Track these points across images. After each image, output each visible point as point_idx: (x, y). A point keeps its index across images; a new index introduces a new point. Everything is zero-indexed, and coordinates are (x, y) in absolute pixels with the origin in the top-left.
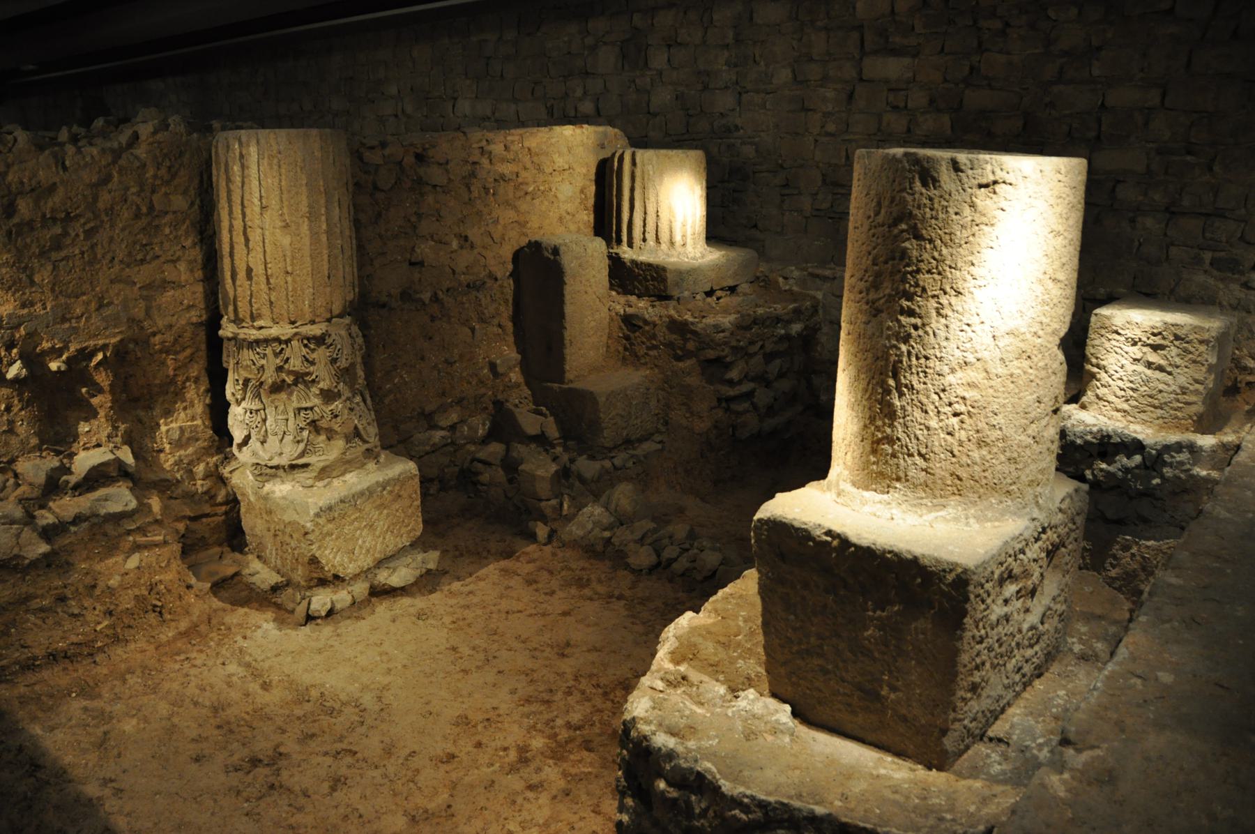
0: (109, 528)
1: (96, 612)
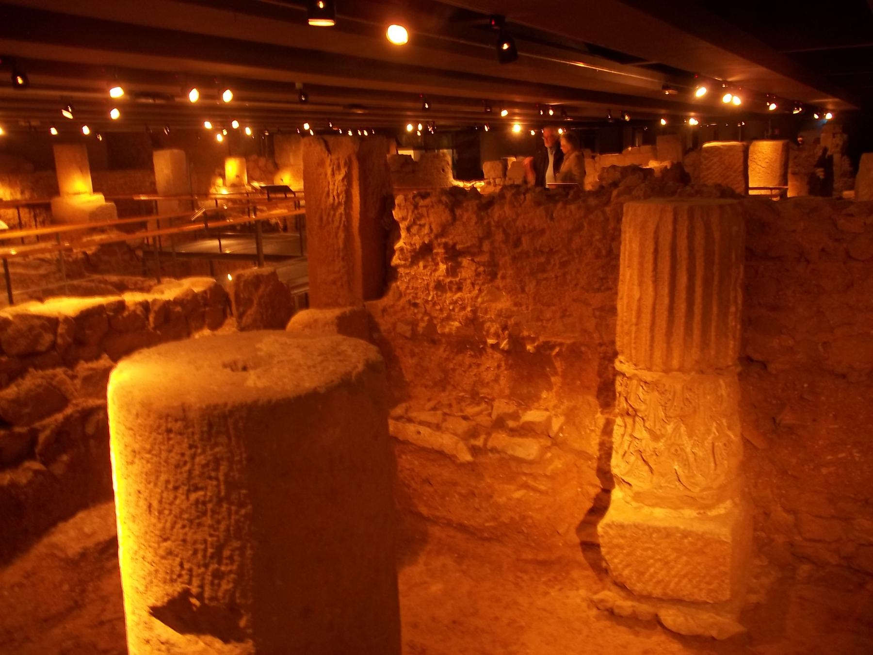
0: (513, 464)
1: (487, 514)
